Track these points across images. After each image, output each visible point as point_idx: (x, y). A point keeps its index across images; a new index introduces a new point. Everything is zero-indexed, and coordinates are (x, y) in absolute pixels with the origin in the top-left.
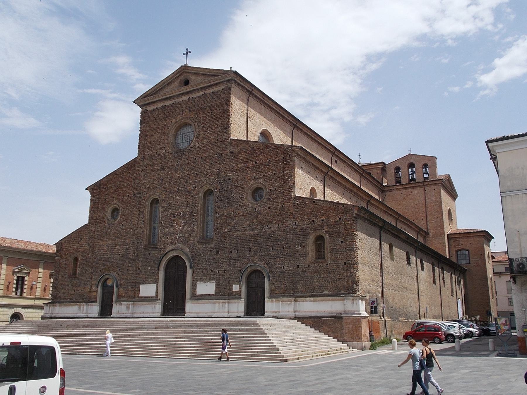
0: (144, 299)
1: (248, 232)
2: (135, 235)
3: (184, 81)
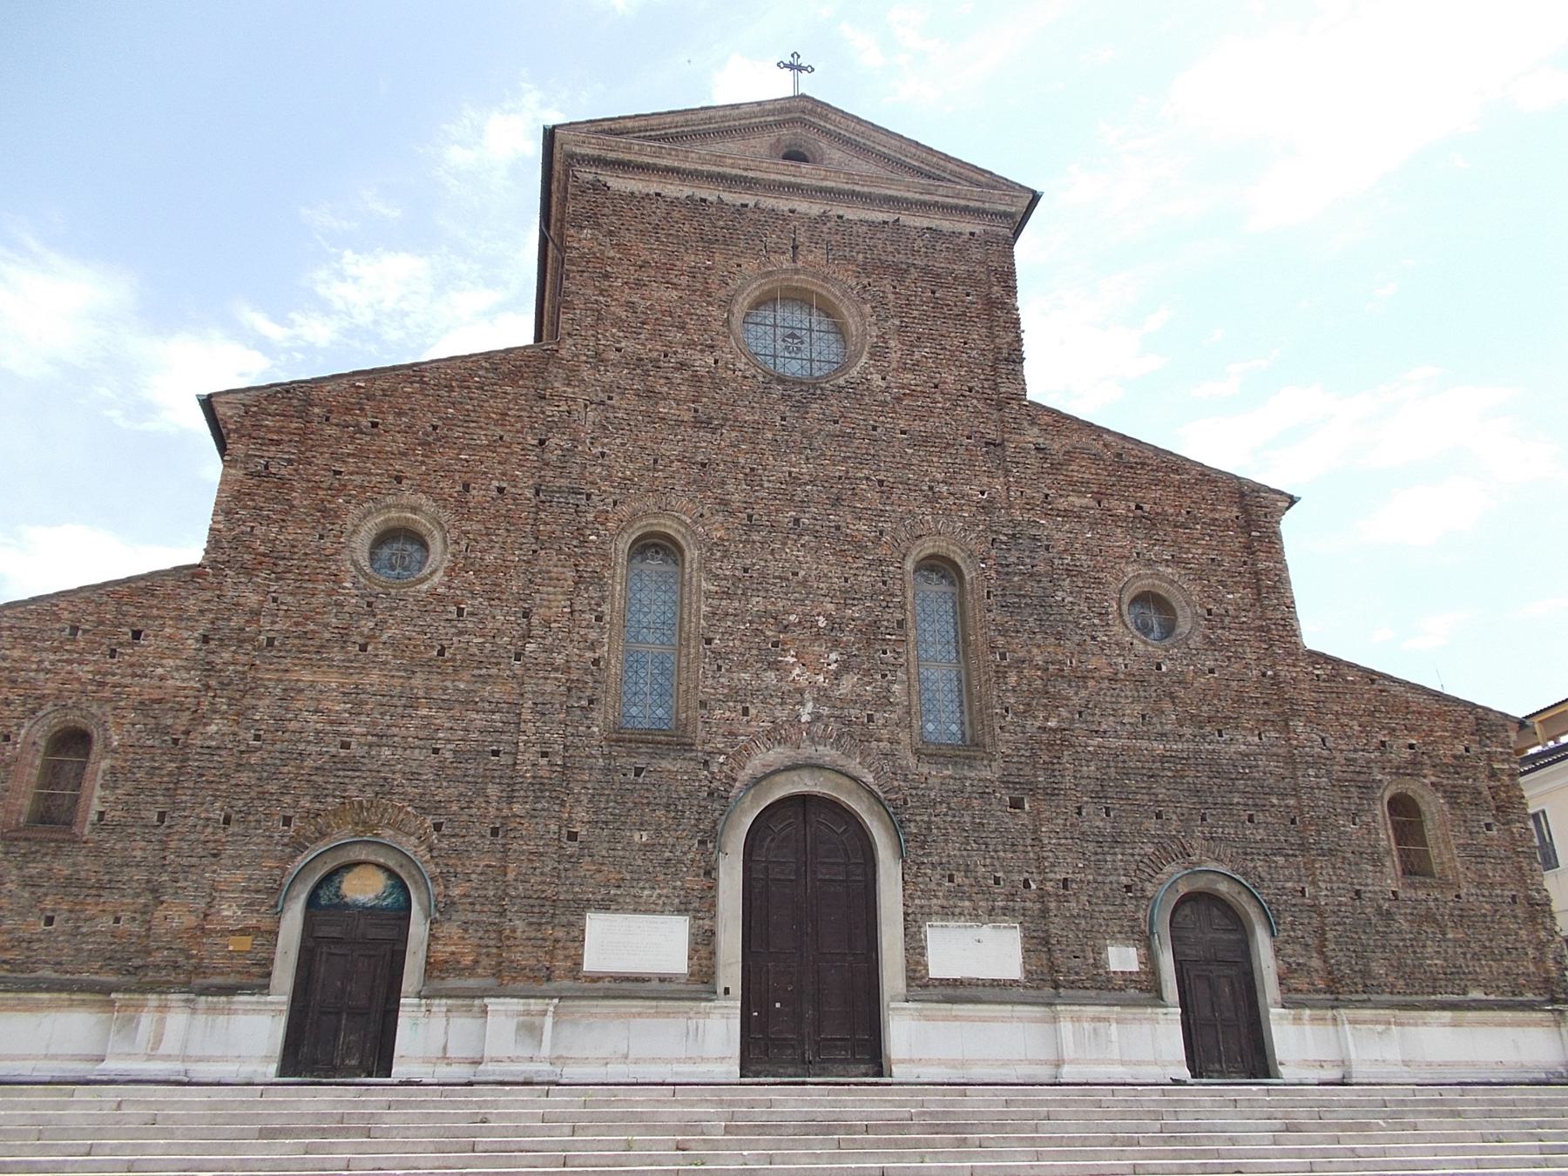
0: (613, 985)
1: (1145, 744)
2: (556, 670)
3: (785, 150)
